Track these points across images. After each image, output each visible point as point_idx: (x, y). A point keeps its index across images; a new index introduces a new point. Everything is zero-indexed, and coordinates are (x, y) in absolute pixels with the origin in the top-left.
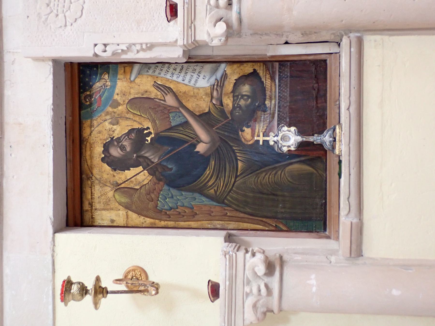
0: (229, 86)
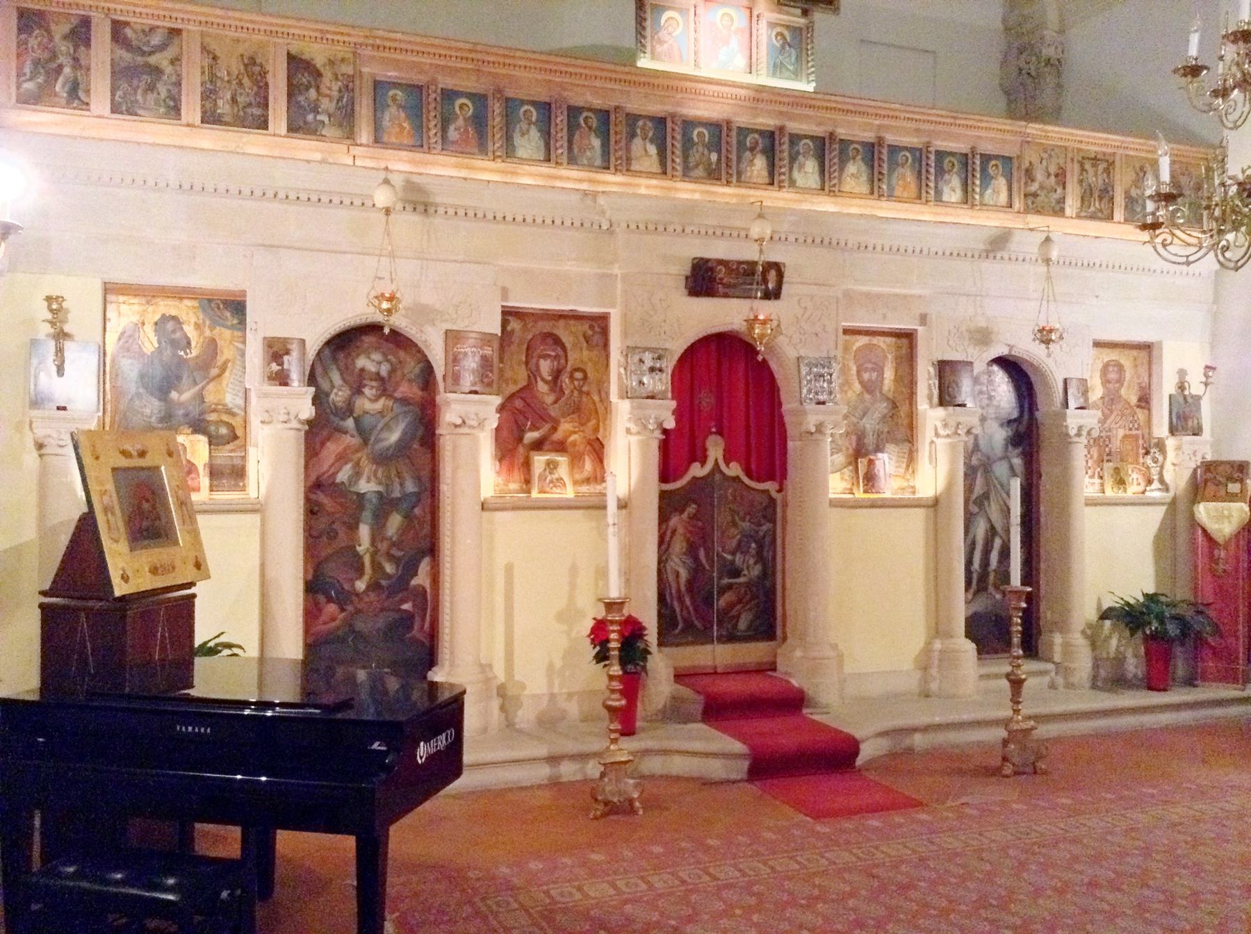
0: (225, 418)
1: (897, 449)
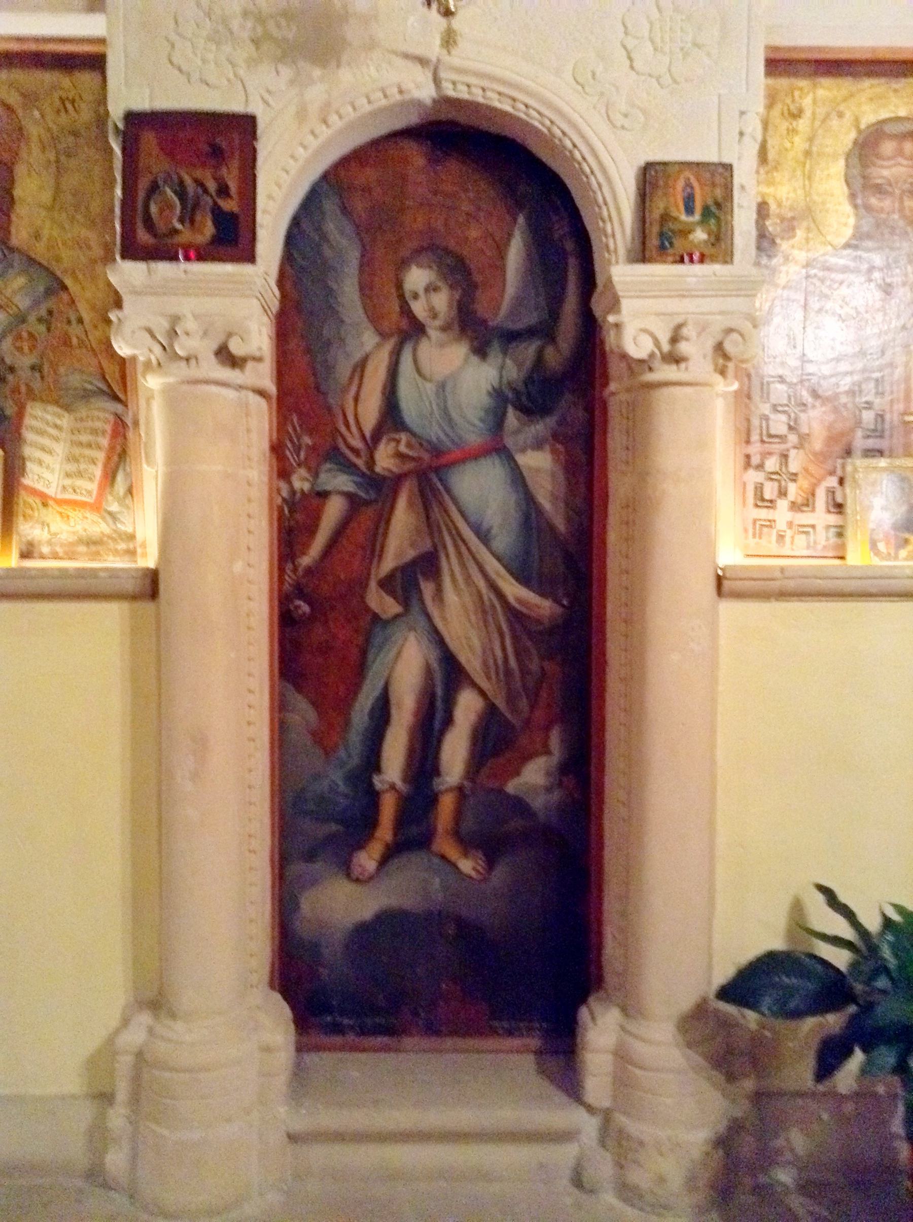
1: (65, 421)
